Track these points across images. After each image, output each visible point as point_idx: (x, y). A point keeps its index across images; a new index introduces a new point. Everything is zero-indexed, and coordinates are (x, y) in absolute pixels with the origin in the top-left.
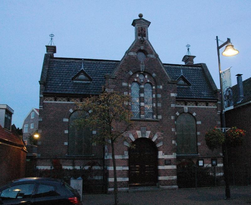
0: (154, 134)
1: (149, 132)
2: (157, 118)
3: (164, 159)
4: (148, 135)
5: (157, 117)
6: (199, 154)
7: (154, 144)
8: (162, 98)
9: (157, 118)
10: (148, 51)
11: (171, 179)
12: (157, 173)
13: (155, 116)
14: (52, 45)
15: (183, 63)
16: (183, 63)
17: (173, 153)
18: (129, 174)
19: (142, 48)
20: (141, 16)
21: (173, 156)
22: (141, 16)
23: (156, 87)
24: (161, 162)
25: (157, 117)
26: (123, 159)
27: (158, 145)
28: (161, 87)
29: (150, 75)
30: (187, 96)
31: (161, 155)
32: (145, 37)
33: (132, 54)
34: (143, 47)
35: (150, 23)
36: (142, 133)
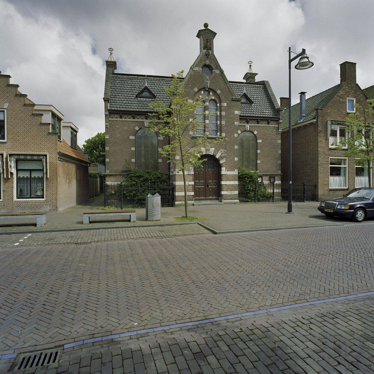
0: (218, 151)
1: (213, 149)
2: (221, 135)
3: (226, 175)
4: (212, 151)
5: (221, 134)
6: (258, 171)
7: (217, 161)
8: (226, 116)
9: (221, 135)
10: (213, 66)
11: (233, 194)
12: (219, 187)
13: (219, 134)
14: (112, 60)
15: (244, 81)
16: (244, 81)
17: (236, 170)
18: (195, 189)
19: (208, 62)
20: (206, 25)
21: (236, 172)
22: (206, 25)
23: (220, 105)
24: (223, 178)
25: (221, 134)
26: (188, 174)
27: (221, 162)
28: (225, 104)
29: (215, 92)
30: (249, 114)
31: (224, 171)
32: (210, 50)
33: (196, 69)
34: (208, 61)
35: (216, 34)
36: (207, 150)
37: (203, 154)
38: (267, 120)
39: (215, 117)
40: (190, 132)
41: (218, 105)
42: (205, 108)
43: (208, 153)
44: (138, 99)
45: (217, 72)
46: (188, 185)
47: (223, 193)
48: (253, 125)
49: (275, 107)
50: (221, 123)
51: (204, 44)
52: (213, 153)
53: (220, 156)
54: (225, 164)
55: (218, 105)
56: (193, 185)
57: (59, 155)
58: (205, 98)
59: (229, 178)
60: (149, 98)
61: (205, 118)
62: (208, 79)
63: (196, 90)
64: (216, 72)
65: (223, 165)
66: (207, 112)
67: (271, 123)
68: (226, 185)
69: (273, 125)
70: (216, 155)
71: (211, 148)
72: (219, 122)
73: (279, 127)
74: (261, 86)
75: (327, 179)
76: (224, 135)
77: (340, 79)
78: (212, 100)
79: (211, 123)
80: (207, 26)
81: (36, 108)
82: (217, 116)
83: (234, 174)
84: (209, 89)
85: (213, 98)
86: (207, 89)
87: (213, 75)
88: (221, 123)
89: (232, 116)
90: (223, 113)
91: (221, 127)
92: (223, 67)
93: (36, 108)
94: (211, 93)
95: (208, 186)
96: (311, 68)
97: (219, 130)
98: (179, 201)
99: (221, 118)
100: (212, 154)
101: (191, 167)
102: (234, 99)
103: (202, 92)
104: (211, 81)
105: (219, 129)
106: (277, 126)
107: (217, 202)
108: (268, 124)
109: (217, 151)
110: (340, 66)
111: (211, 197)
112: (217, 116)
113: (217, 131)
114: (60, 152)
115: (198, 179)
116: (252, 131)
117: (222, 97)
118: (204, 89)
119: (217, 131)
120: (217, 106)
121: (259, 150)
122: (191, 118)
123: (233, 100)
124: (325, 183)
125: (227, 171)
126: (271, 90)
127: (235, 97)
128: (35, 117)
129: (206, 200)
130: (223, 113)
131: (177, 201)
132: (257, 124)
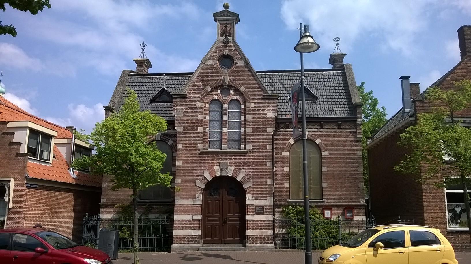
0: (240, 170)
1: (233, 168)
2: (245, 148)
3: (253, 205)
4: (230, 171)
5: (245, 146)
6: (324, 200)
7: (239, 184)
8: (253, 121)
9: (245, 148)
10: (235, 55)
11: (264, 234)
12: (243, 225)
13: (243, 146)
14: (145, 58)
15: (331, 66)
16: (331, 66)
17: (268, 198)
18: (204, 225)
19: (226, 52)
20: (226, 7)
21: (267, 202)
22: (226, 7)
23: (245, 106)
24: (248, 210)
25: (245, 146)
26: (193, 205)
27: (245, 186)
28: (253, 105)
29: (237, 91)
30: (327, 115)
31: (249, 200)
32: (230, 36)
33: (211, 62)
34: (227, 51)
36: (221, 170)
37: (217, 175)
38: (337, 122)
39: (238, 123)
40: (199, 145)
41: (243, 106)
42: (223, 112)
43: (224, 174)
44: (153, 104)
45: (240, 63)
46: (193, 220)
47: (248, 232)
48: (313, 130)
49: (351, 101)
50: (245, 131)
51: (222, 29)
52: (232, 173)
53: (243, 178)
54: (251, 189)
55: (243, 106)
56: (199, 220)
57: (27, 180)
58: (223, 98)
59: (185, 209)
60: (167, 103)
61: (222, 124)
62: (226, 74)
63: (209, 89)
64: (239, 64)
65: (248, 191)
66: (225, 118)
67: (344, 125)
68: (253, 220)
69: (346, 130)
70: (236, 175)
71: (229, 167)
72: (243, 130)
73: (358, 131)
74: (339, 72)
75: (442, 214)
76: (249, 147)
77: (460, 52)
78: (214, 100)
79: (233, 131)
80: (228, 7)
81: (9, 125)
82: (240, 122)
83: (266, 204)
84: (229, 86)
85: (235, 97)
86: (226, 87)
87: (235, 67)
88: (245, 131)
89: (263, 120)
90: (249, 117)
91: (245, 136)
92: (247, 56)
93: (9, 125)
94: (232, 92)
95: (225, 222)
96: (316, 51)
97: (243, 140)
98: (177, 244)
99: (245, 124)
100: (231, 175)
101: (197, 193)
102: (265, 97)
103: (219, 91)
104: (230, 76)
105: (244, 139)
106: (354, 130)
107: (239, 246)
108: (339, 127)
109: (238, 170)
110: (457, 33)
111: (231, 239)
112: (240, 122)
113: (240, 143)
114: (29, 176)
115: (218, 212)
116: (312, 139)
117: (248, 96)
118: (221, 87)
119: (240, 143)
120: (240, 108)
121: (325, 167)
122: (200, 127)
123: (264, 98)
124: (439, 219)
125: (255, 199)
126: (353, 77)
127: (267, 95)
128: (5, 136)
129: (221, 242)
130: (249, 117)
131: (174, 244)
132: (320, 128)
